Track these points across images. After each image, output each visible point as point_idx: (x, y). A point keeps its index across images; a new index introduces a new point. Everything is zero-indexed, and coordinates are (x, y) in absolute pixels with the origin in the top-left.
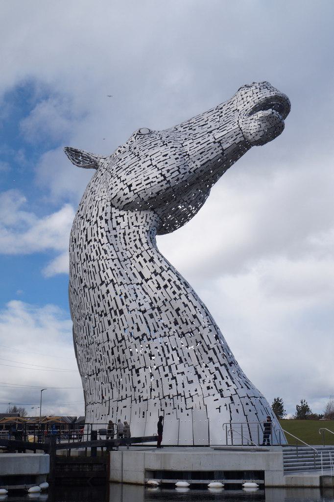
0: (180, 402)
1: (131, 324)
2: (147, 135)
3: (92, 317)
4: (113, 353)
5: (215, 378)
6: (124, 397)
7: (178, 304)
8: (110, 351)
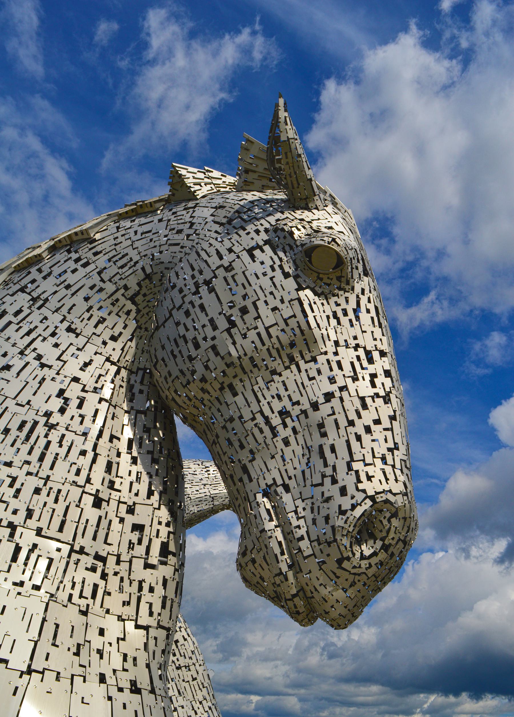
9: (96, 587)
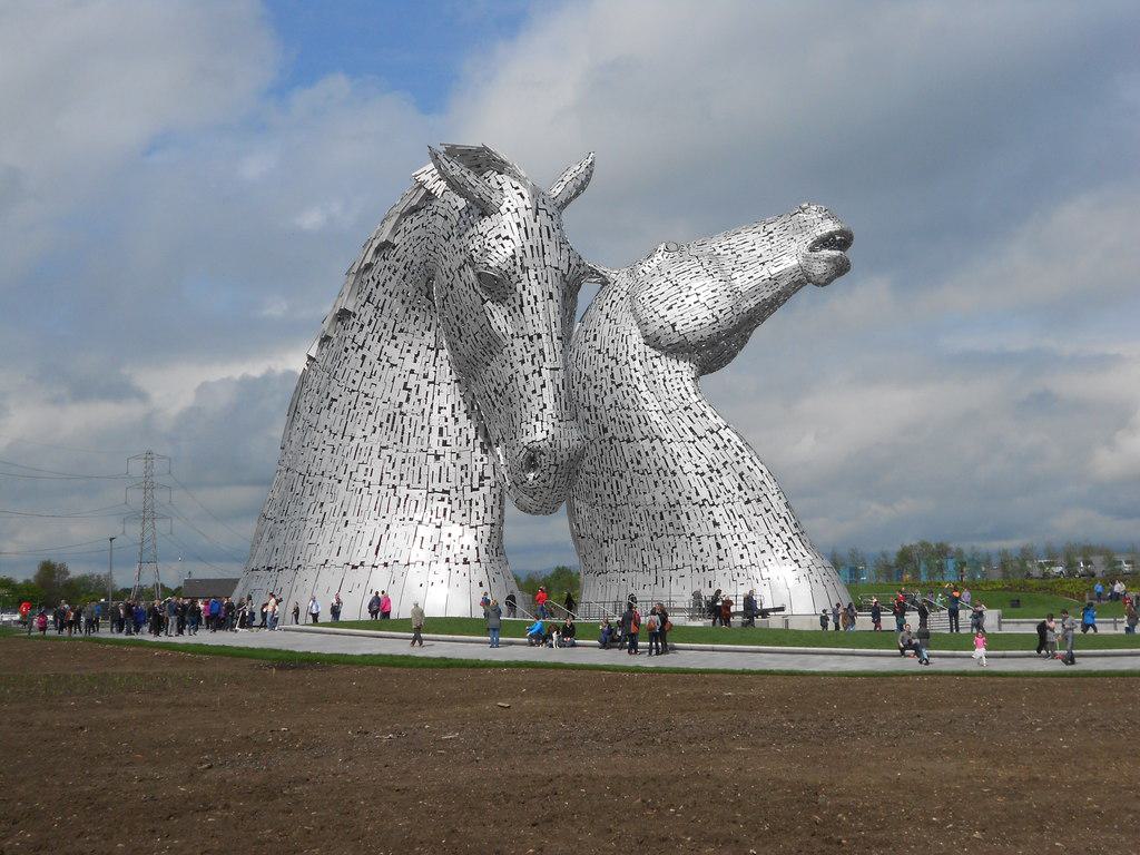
0: (754, 572)
1: (687, 488)
2: (676, 253)
3: (627, 474)
4: (662, 518)
5: (789, 548)
6: (680, 565)
7: (743, 468)
8: (658, 517)
9: (445, 509)
